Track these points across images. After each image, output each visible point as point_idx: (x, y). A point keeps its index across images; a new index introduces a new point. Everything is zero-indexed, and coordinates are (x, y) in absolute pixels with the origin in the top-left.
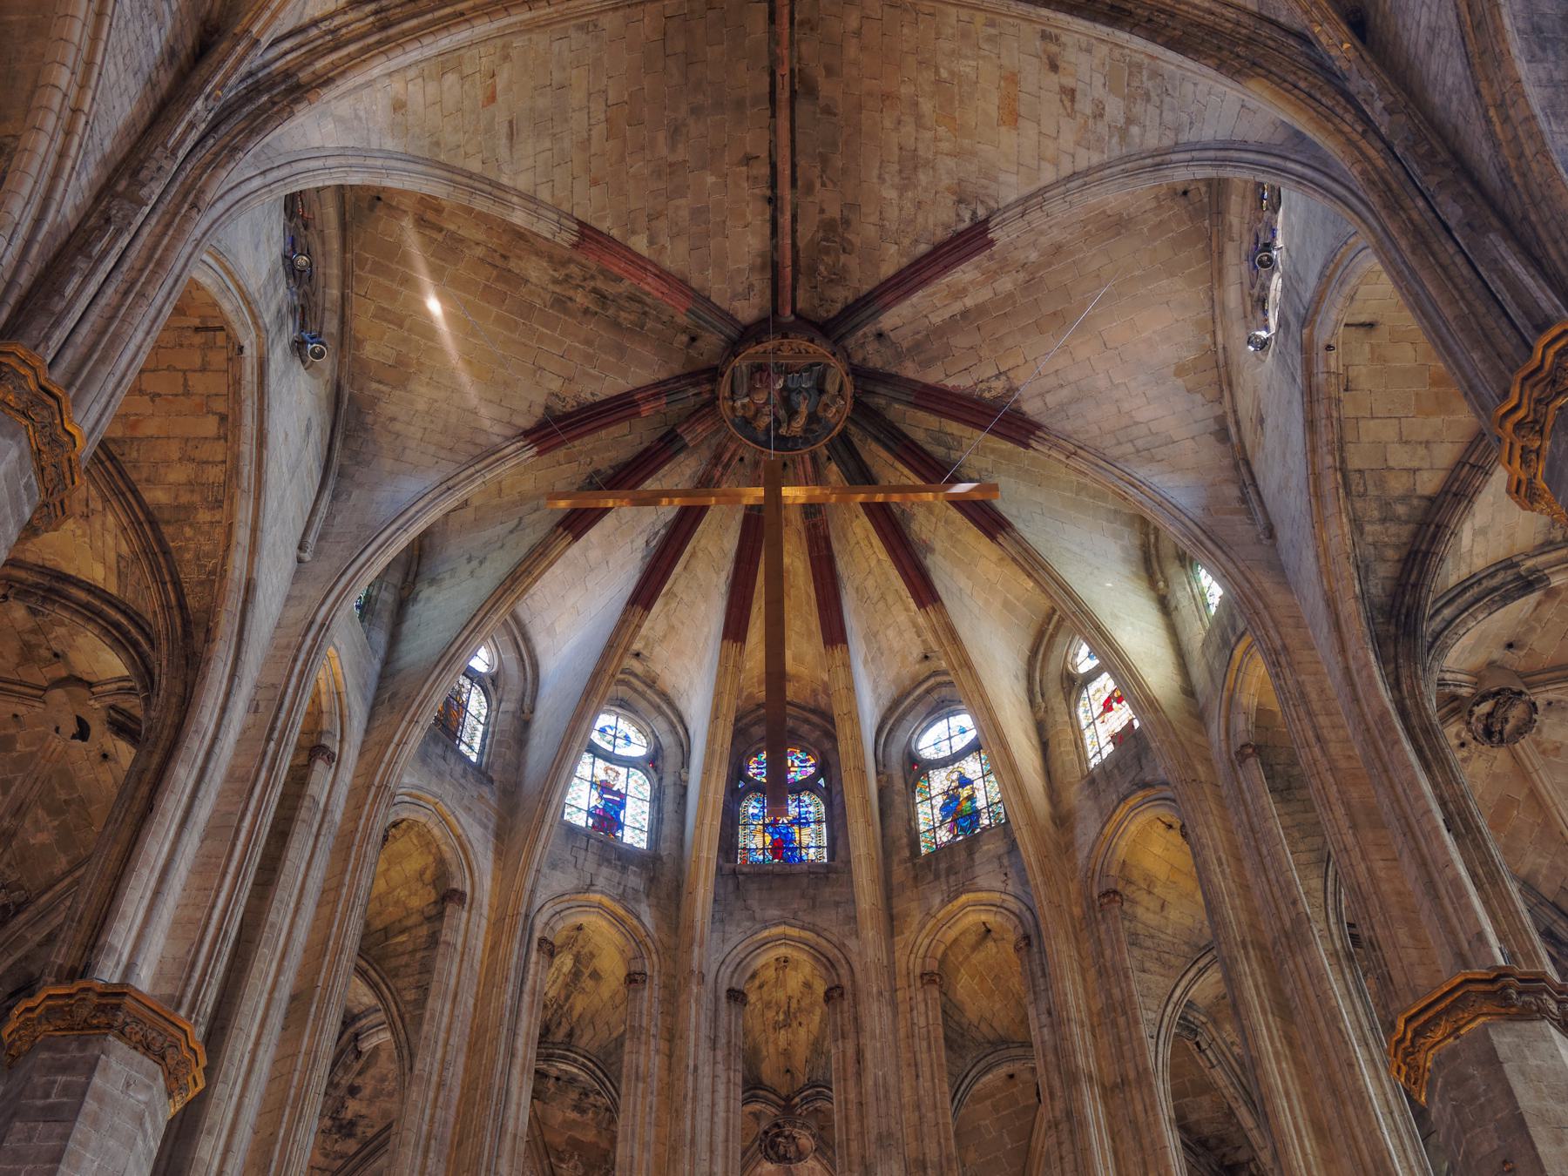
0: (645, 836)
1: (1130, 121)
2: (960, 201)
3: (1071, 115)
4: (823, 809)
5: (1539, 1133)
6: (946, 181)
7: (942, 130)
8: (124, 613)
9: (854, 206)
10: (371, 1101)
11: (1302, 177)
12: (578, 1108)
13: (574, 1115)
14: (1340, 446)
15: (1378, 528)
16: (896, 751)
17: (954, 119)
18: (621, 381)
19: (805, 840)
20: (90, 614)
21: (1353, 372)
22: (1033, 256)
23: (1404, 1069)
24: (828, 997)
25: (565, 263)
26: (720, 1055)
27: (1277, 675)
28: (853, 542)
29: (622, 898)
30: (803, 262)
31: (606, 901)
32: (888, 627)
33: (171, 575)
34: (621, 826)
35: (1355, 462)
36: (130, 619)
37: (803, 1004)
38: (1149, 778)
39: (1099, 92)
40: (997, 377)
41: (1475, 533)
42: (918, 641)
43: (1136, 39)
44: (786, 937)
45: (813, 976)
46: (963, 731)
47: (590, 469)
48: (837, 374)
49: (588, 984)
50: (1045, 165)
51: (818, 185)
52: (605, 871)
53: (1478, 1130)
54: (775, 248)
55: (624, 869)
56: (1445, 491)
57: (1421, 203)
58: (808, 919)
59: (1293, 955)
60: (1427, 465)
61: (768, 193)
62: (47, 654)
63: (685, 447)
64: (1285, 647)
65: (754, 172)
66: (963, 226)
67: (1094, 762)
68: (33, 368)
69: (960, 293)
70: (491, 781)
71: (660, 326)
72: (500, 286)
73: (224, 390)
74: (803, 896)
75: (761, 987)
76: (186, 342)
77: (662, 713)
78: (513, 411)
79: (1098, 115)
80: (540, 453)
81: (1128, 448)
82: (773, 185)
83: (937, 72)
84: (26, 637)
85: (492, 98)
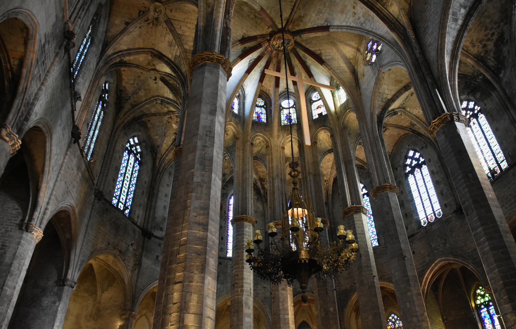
1: (364, 23)
3: (353, 17)
5: (393, 210)
6: (325, 17)
7: (328, 9)
9: (306, 15)
24: (266, 147)
29: (236, 124)
39: (361, 15)
40: (319, 50)
48: (293, 41)
55: (236, 118)
56: (391, 99)
57: (421, 73)
58: (264, 133)
62: (152, 64)
66: (324, 25)
67: (314, 118)
78: (237, 35)
79: (359, 19)
81: (339, 71)
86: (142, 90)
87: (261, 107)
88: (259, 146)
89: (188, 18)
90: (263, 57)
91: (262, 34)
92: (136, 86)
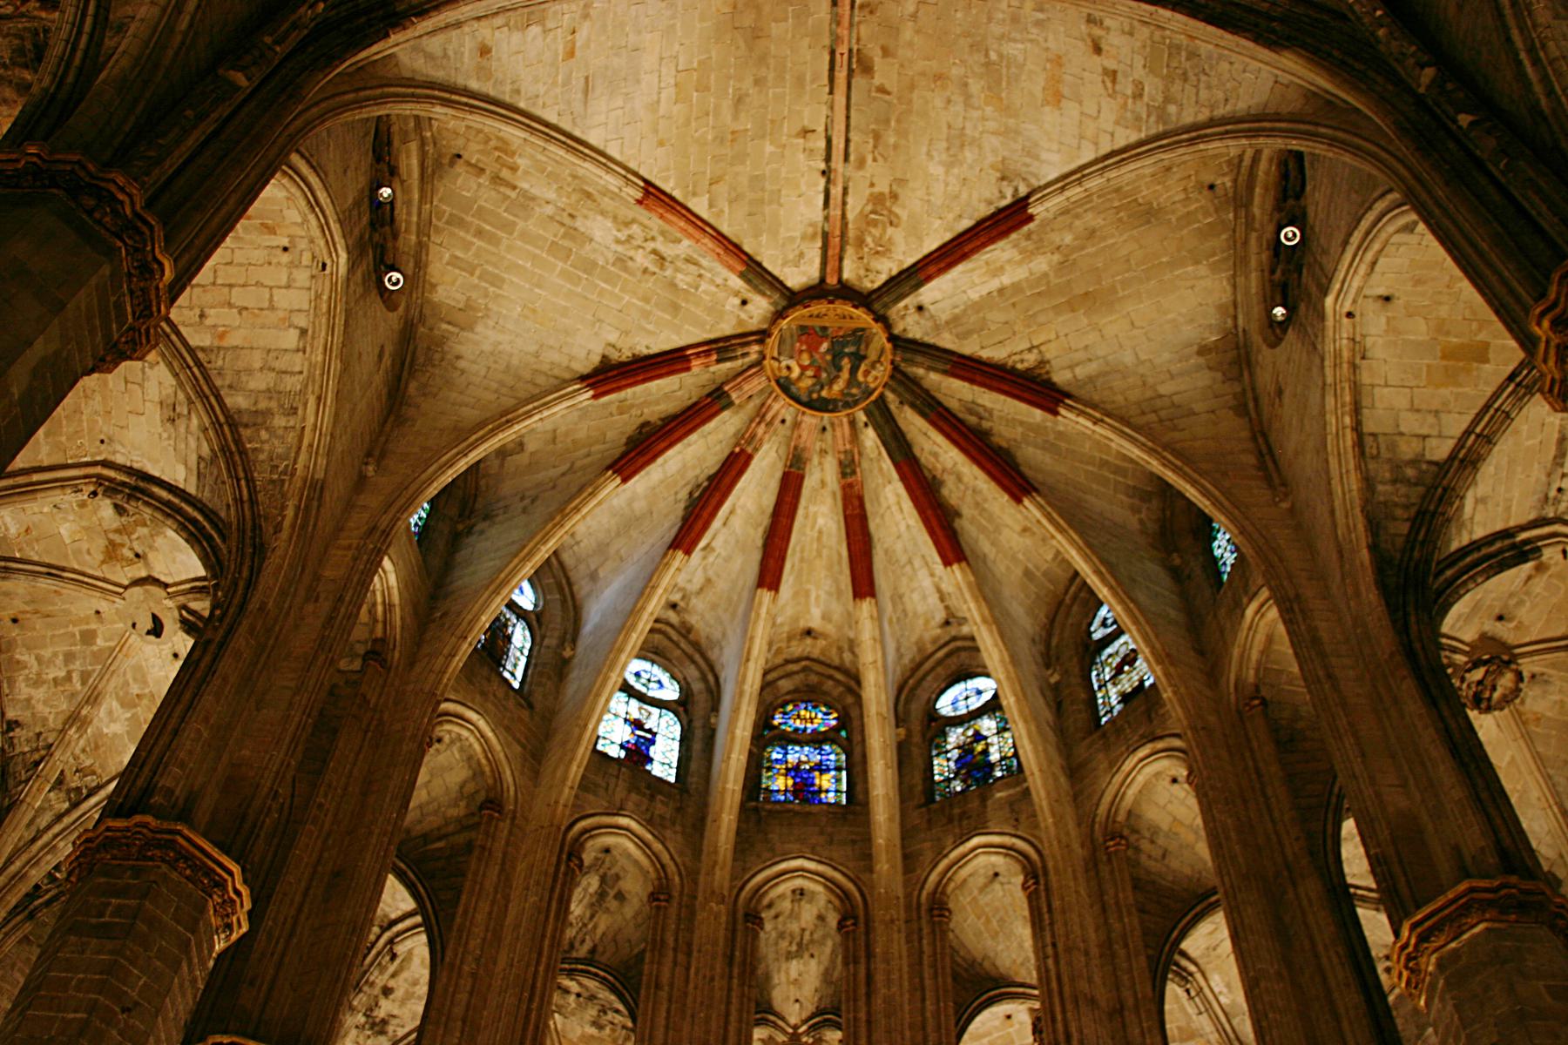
0: (674, 772)
1: (1168, 100)
2: (1003, 178)
4: (843, 757)
6: (990, 159)
7: (989, 110)
8: (201, 511)
9: (902, 182)
10: (403, 1002)
11: (1333, 139)
12: (596, 1024)
13: (593, 1031)
14: (1357, 409)
15: (1389, 488)
16: (917, 708)
17: (1001, 99)
18: (674, 337)
19: (825, 785)
20: (169, 511)
21: (1369, 342)
22: (1068, 238)
23: (1405, 974)
25: (627, 224)
26: (736, 971)
27: (1291, 621)
28: (884, 505)
29: (649, 823)
30: (851, 233)
31: (634, 825)
32: (912, 591)
33: (245, 470)
34: (651, 760)
35: (1369, 426)
36: (206, 516)
37: (816, 936)
38: (1159, 732)
39: (1139, 72)
40: (1030, 350)
41: (1477, 501)
42: (941, 606)
43: (1179, 16)
44: (803, 870)
45: (827, 909)
46: (979, 692)
47: (641, 420)
48: (880, 338)
49: (613, 904)
50: (1085, 143)
51: (869, 158)
52: (634, 797)
53: (1477, 1026)
54: (827, 218)
56: (1452, 457)
57: (1451, 145)
59: (1295, 885)
60: (1435, 433)
61: (823, 166)
62: (131, 555)
63: (730, 404)
64: (1298, 596)
65: (810, 145)
66: (1004, 203)
68: (130, 196)
69: (1000, 270)
70: (531, 706)
71: (714, 289)
72: (566, 243)
73: (306, 307)
74: (821, 833)
75: (776, 917)
76: (274, 261)
77: (693, 662)
78: (572, 358)
79: (1138, 95)
80: (595, 397)
81: (1153, 417)
82: (828, 159)
83: (987, 55)
84: (111, 536)
85: (571, 54)
86: (110, 704)
87: (817, 740)
88: (822, 942)
89: (230, 263)
90: (750, 458)
91: (712, 336)
92: (78, 686)
